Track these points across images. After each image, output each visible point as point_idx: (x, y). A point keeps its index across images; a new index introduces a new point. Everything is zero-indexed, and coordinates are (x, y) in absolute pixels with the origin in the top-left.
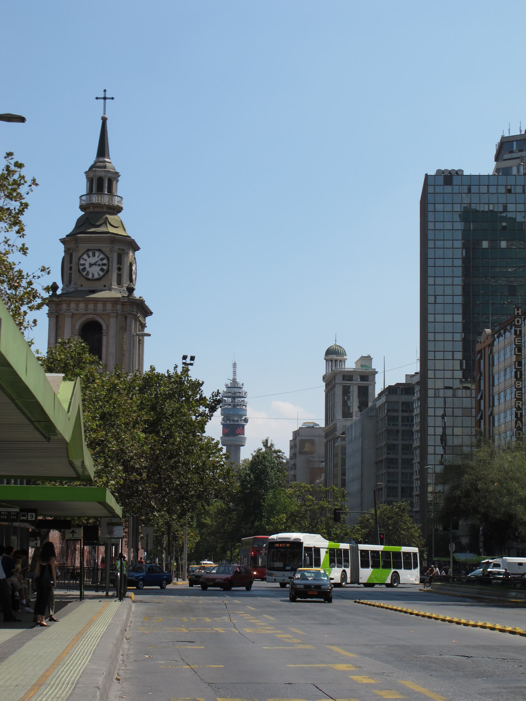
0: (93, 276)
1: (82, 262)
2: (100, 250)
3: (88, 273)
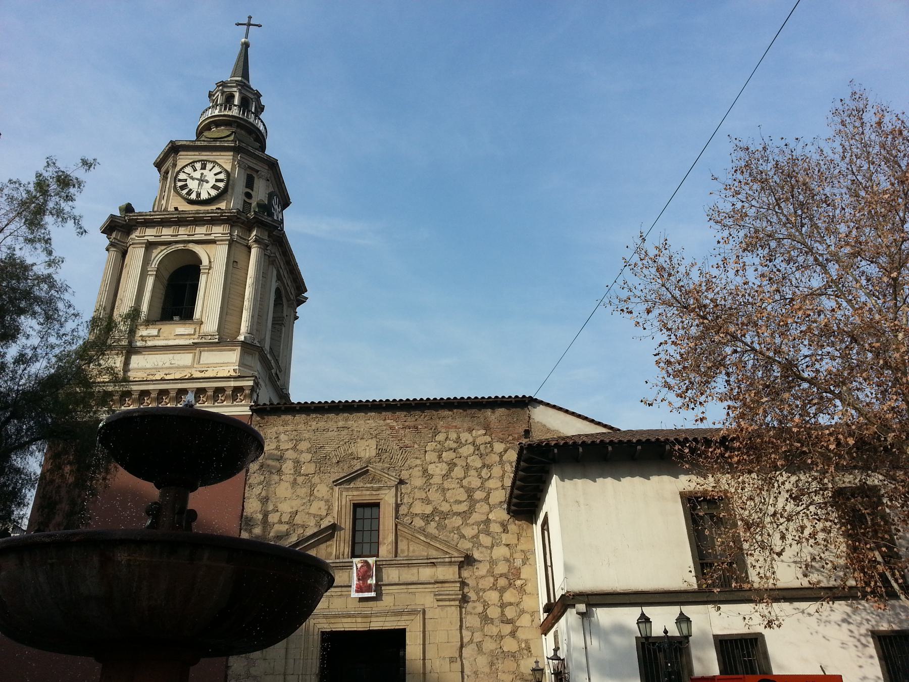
0: (199, 195)
1: (182, 176)
3: (190, 192)
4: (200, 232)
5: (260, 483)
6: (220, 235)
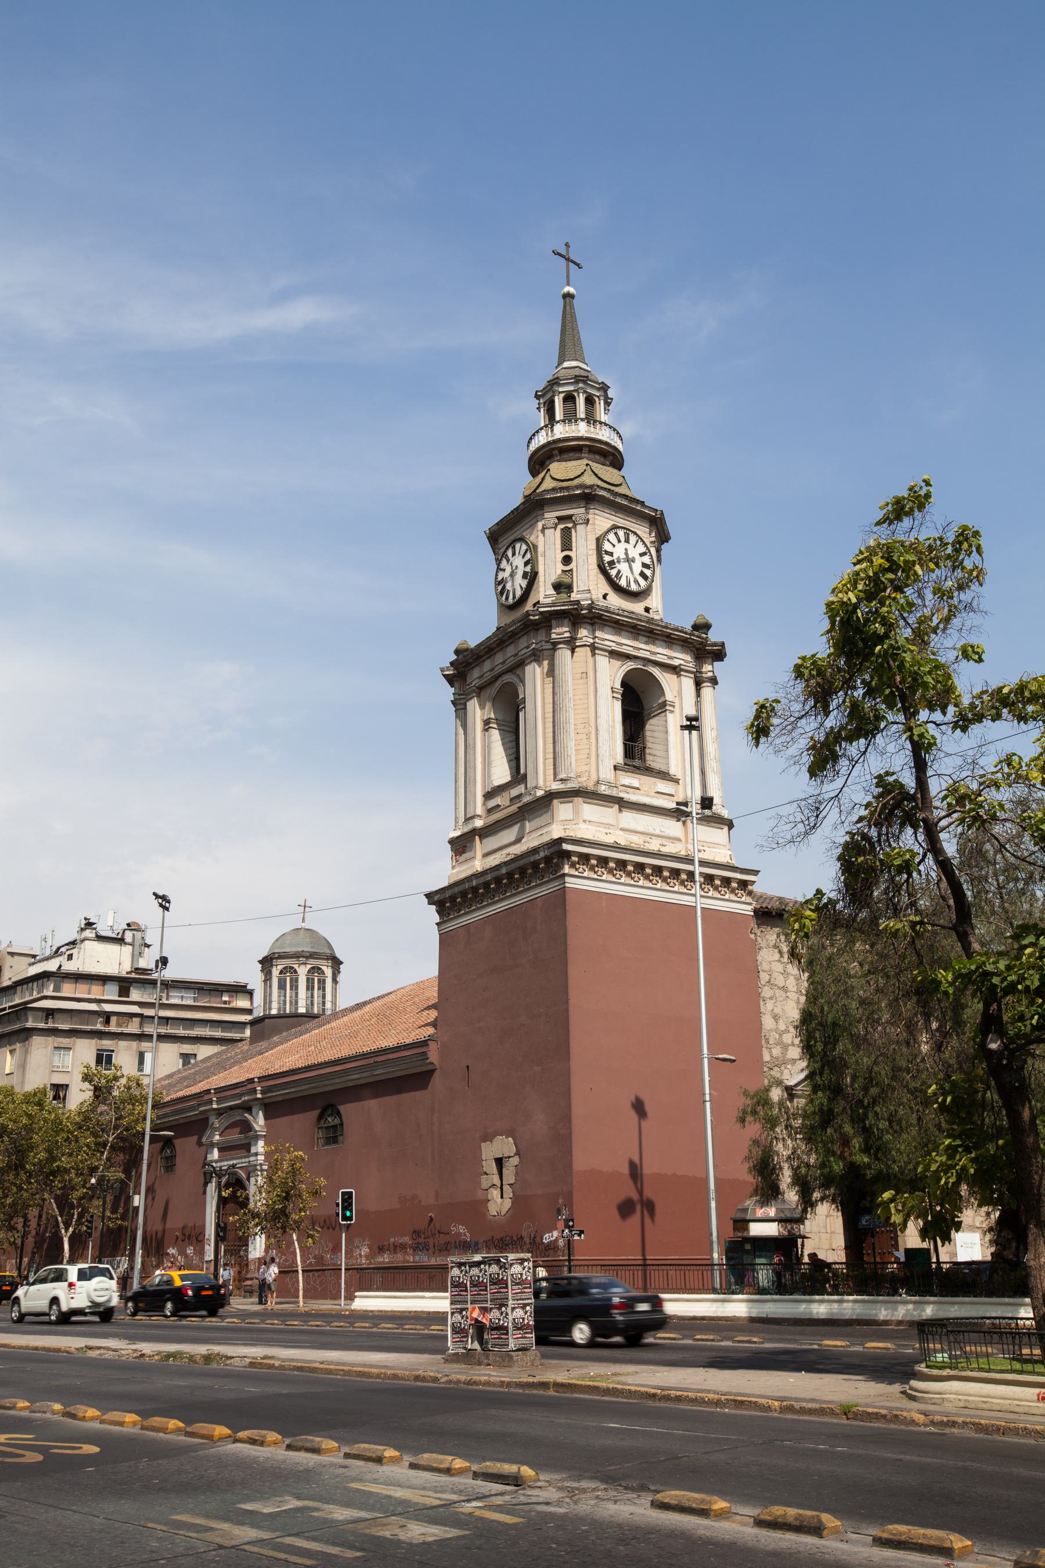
0: (629, 584)
2: (635, 533)
4: (662, 653)
5: (771, 998)
6: (682, 662)
